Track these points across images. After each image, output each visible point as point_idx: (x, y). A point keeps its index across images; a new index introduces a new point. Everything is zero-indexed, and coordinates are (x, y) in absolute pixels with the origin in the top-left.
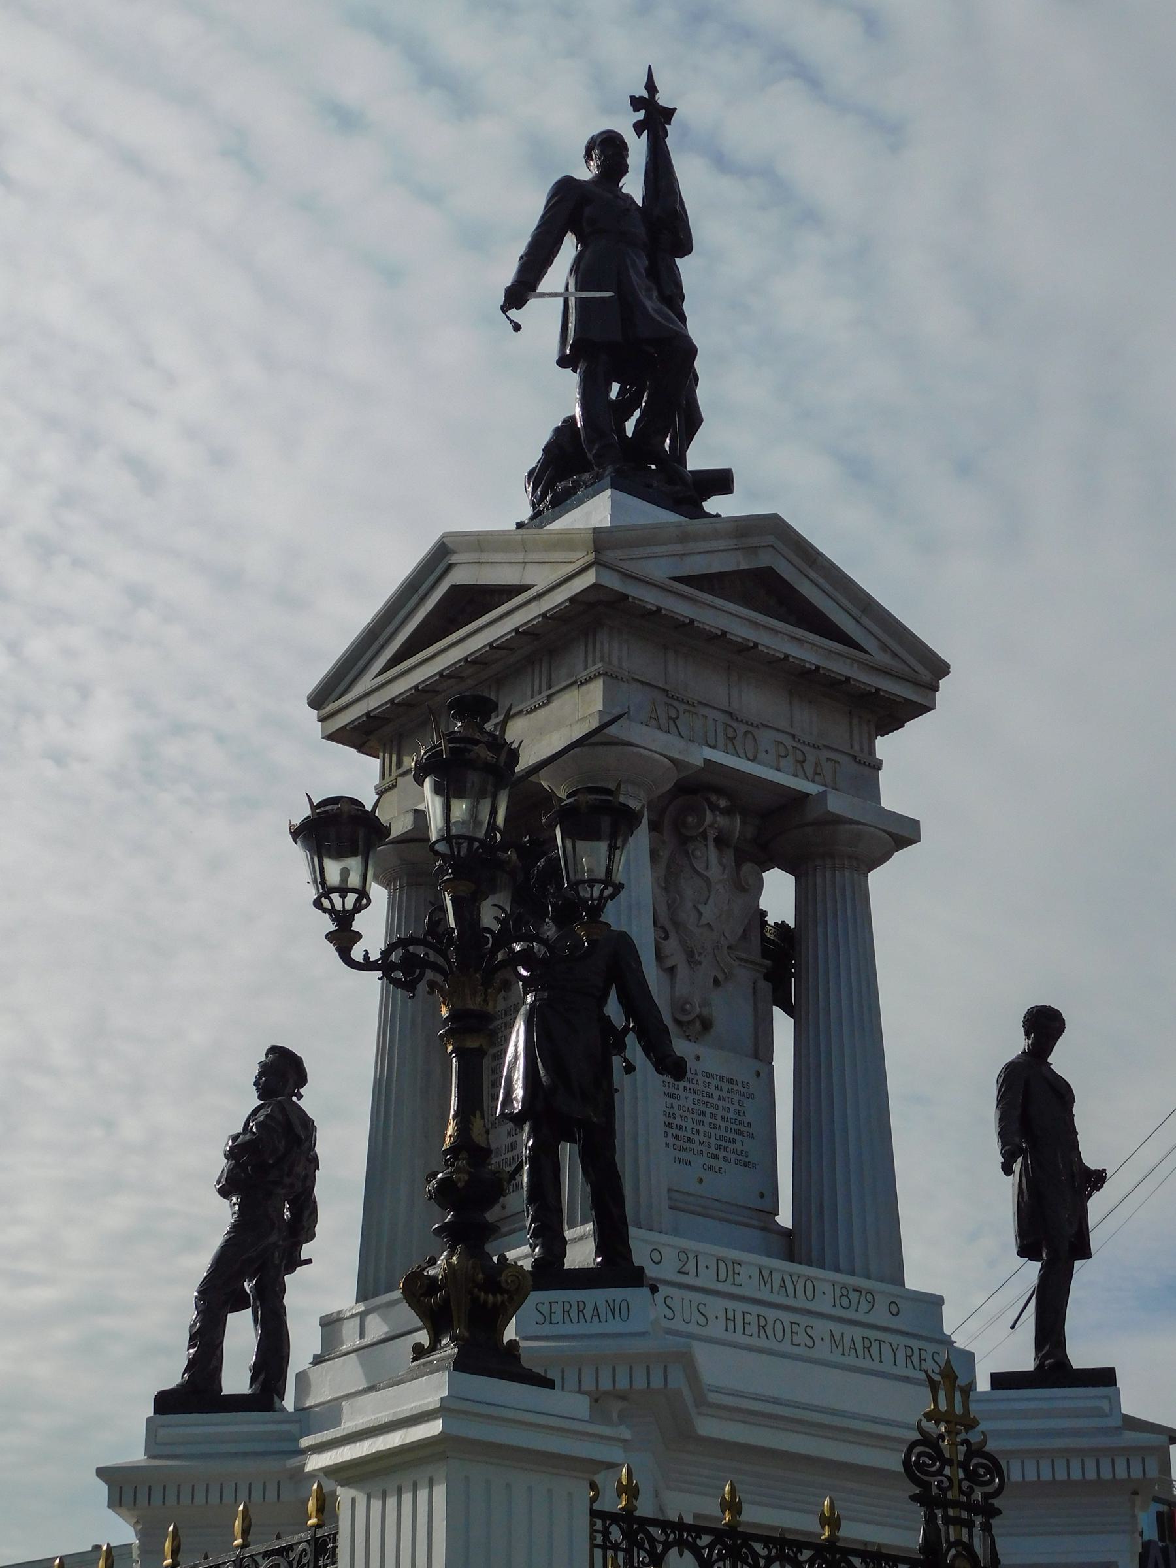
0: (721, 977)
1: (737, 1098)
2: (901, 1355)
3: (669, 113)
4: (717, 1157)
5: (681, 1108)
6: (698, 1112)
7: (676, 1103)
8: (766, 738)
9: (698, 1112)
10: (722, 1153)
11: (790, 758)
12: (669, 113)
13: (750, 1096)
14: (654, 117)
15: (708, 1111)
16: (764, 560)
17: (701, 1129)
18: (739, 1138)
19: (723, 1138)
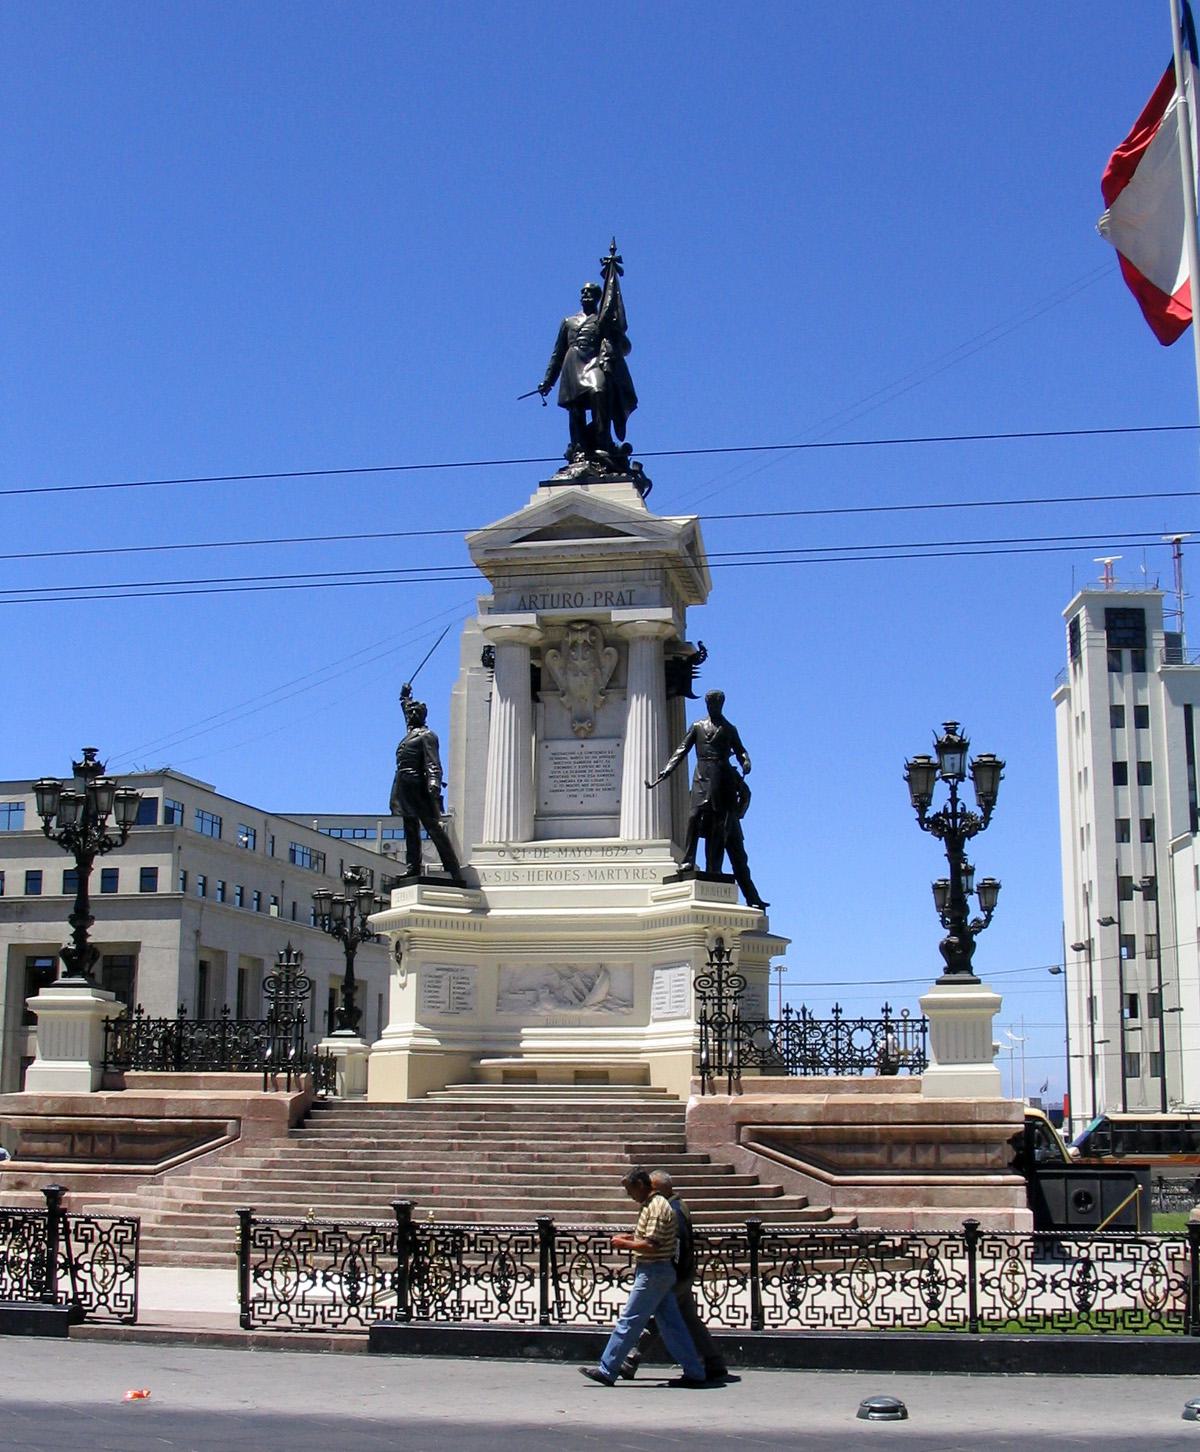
0: (598, 706)
1: (605, 759)
2: (631, 875)
3: (619, 260)
4: (592, 790)
5: (571, 772)
6: (581, 772)
7: (568, 770)
8: (588, 594)
9: (581, 772)
10: (594, 788)
11: (604, 598)
12: (619, 260)
13: (613, 757)
14: (612, 267)
15: (587, 769)
16: (568, 513)
17: (583, 779)
18: (604, 778)
19: (596, 780)
